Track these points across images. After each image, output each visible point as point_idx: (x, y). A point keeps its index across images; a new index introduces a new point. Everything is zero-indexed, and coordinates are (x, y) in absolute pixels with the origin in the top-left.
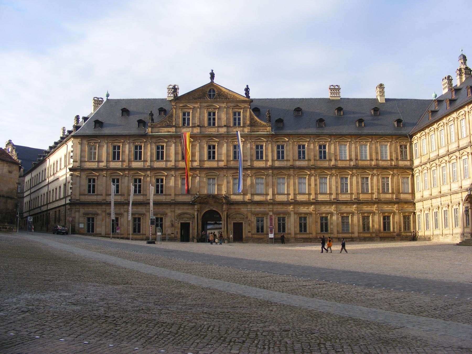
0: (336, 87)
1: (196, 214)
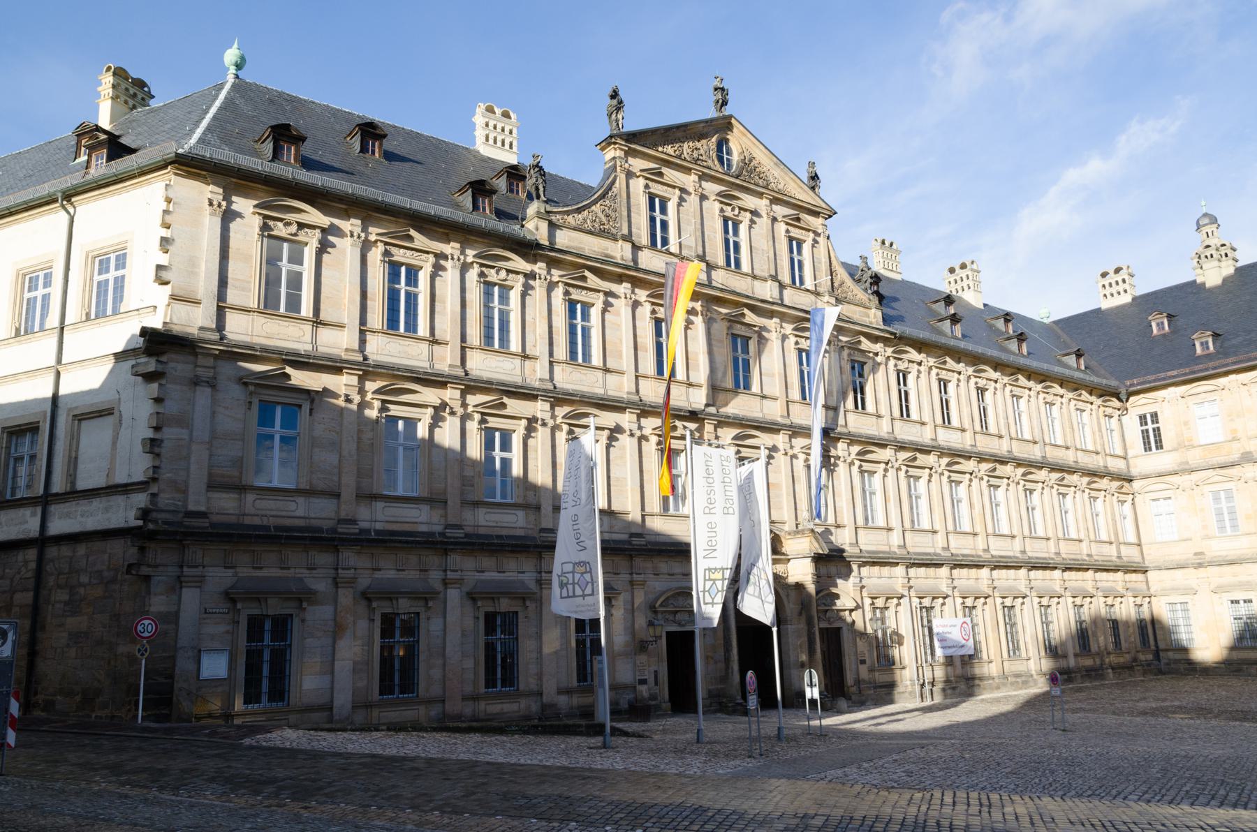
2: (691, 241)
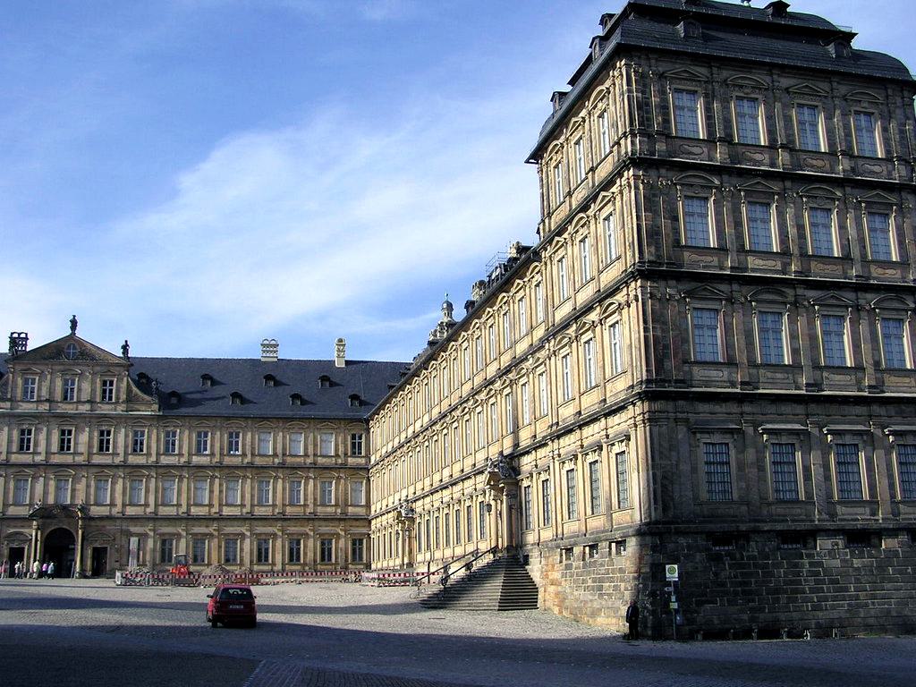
0: (273, 342)
1: (34, 534)
2: (44, 393)
